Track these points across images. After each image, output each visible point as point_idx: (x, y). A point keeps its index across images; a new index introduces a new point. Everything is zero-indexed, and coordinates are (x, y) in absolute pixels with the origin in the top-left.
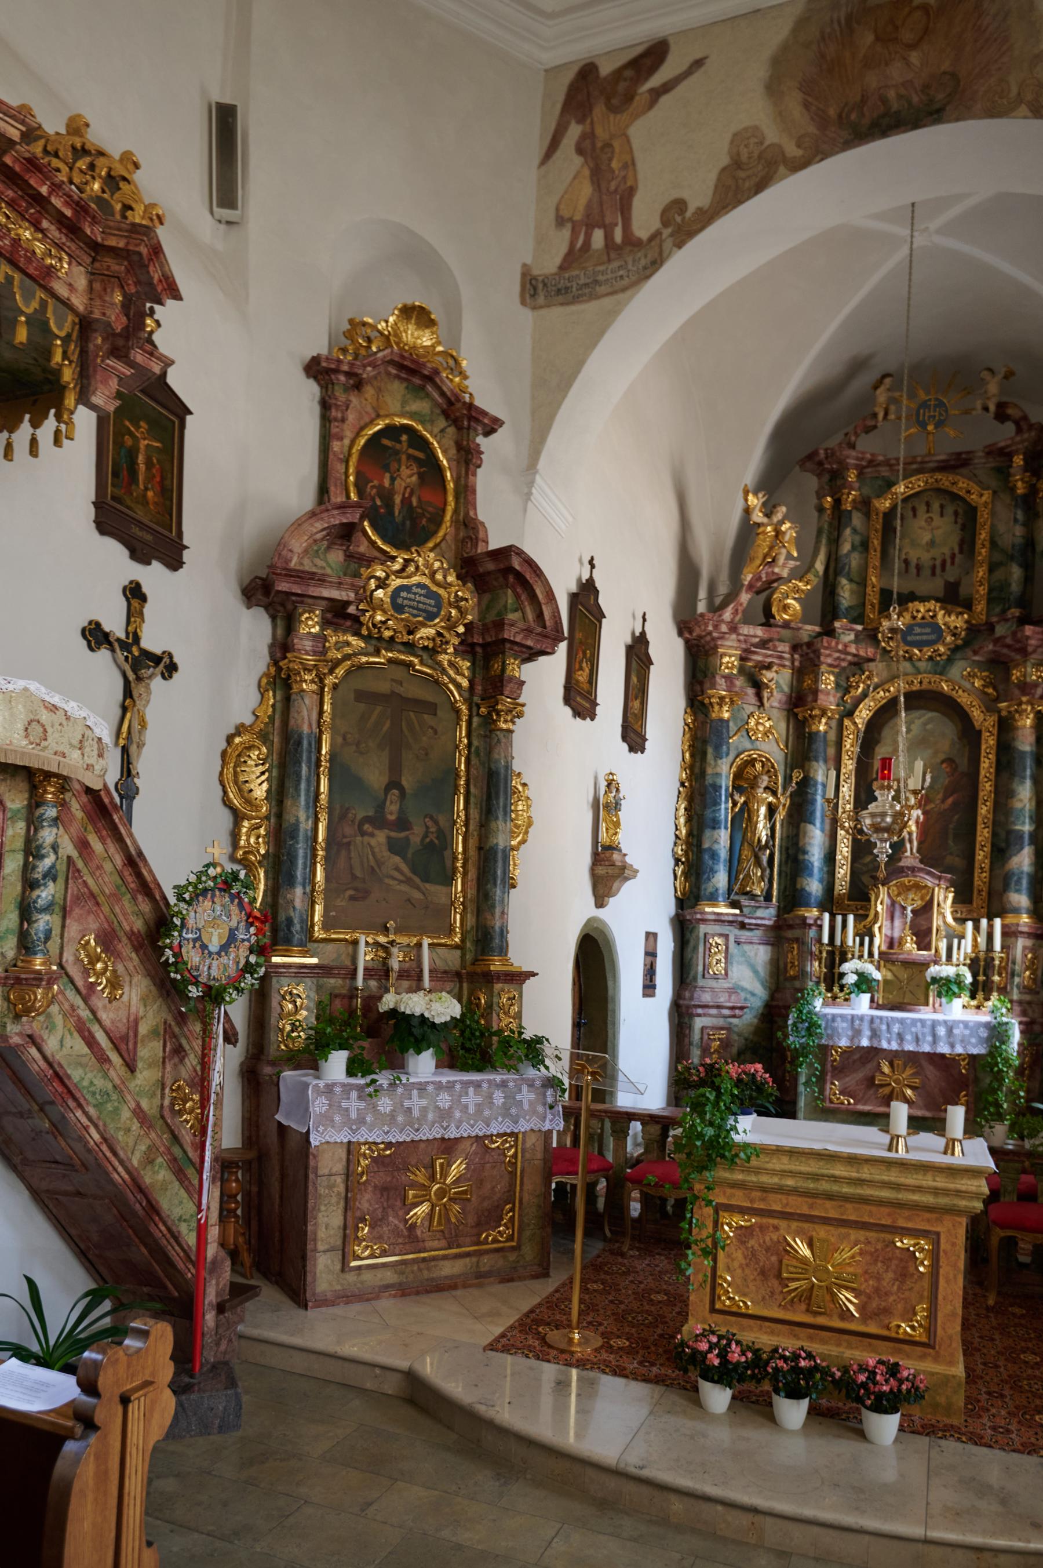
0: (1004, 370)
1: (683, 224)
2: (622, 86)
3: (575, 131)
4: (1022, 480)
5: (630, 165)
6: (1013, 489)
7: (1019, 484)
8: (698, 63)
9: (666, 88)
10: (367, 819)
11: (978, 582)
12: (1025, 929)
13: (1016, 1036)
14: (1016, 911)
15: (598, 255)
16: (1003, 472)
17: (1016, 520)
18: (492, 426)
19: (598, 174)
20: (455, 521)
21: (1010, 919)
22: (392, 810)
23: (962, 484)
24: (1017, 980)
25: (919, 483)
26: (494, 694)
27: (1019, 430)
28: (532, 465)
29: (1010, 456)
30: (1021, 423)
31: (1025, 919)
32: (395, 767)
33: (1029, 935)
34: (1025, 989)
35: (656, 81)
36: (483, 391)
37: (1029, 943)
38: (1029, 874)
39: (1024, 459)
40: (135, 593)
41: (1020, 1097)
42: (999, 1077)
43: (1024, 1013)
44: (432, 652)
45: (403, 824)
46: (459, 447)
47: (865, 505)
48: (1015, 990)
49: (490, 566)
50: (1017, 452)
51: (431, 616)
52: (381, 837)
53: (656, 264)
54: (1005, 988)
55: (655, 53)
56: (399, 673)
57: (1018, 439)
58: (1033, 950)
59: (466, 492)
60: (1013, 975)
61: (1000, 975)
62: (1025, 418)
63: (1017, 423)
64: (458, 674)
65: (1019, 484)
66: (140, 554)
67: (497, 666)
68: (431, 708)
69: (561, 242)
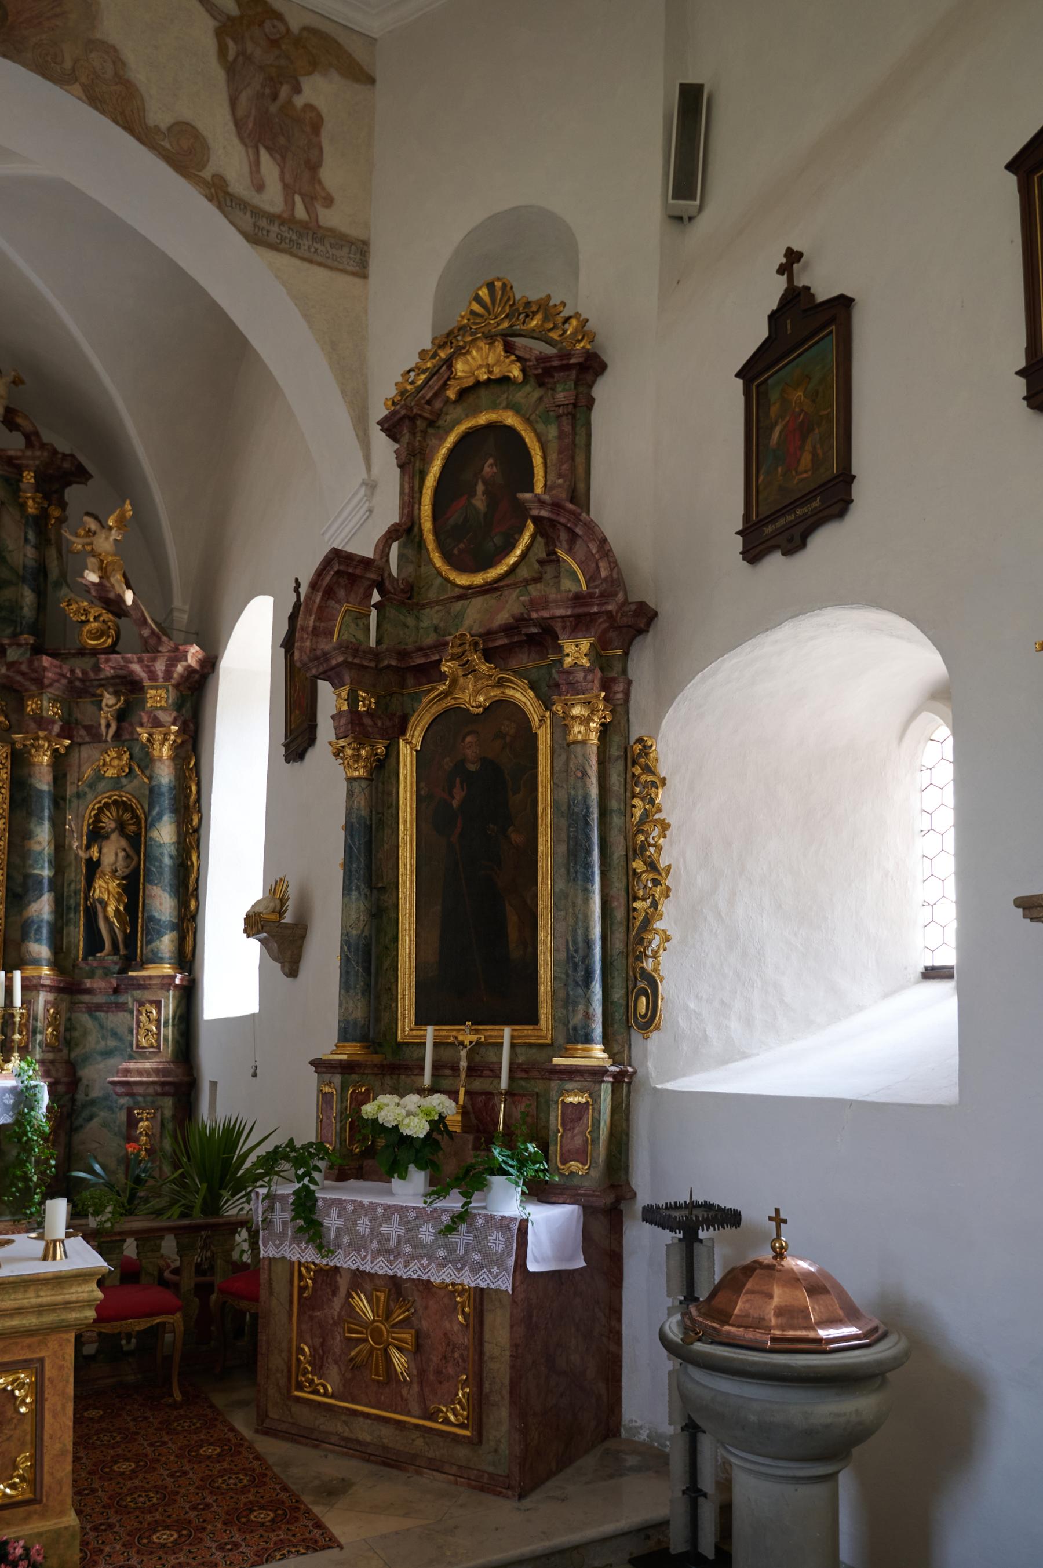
0: (13, 373)
4: (34, 499)
6: (23, 506)
7: (30, 502)
12: (48, 982)
13: (44, 1099)
14: (36, 962)
17: (26, 540)
24: (39, 1037)
27: (29, 444)
29: (19, 469)
30: (31, 439)
31: (46, 971)
33: (51, 989)
34: (48, 1047)
37: (51, 997)
38: (48, 923)
39: (35, 477)
41: (51, 1167)
42: (27, 1148)
43: (46, 1074)
48: (38, 1048)
50: (27, 467)
54: (26, 1047)
57: (29, 453)
58: (55, 1004)
60: (34, 1032)
61: (20, 1033)
62: (37, 434)
63: (27, 437)
65: (30, 502)
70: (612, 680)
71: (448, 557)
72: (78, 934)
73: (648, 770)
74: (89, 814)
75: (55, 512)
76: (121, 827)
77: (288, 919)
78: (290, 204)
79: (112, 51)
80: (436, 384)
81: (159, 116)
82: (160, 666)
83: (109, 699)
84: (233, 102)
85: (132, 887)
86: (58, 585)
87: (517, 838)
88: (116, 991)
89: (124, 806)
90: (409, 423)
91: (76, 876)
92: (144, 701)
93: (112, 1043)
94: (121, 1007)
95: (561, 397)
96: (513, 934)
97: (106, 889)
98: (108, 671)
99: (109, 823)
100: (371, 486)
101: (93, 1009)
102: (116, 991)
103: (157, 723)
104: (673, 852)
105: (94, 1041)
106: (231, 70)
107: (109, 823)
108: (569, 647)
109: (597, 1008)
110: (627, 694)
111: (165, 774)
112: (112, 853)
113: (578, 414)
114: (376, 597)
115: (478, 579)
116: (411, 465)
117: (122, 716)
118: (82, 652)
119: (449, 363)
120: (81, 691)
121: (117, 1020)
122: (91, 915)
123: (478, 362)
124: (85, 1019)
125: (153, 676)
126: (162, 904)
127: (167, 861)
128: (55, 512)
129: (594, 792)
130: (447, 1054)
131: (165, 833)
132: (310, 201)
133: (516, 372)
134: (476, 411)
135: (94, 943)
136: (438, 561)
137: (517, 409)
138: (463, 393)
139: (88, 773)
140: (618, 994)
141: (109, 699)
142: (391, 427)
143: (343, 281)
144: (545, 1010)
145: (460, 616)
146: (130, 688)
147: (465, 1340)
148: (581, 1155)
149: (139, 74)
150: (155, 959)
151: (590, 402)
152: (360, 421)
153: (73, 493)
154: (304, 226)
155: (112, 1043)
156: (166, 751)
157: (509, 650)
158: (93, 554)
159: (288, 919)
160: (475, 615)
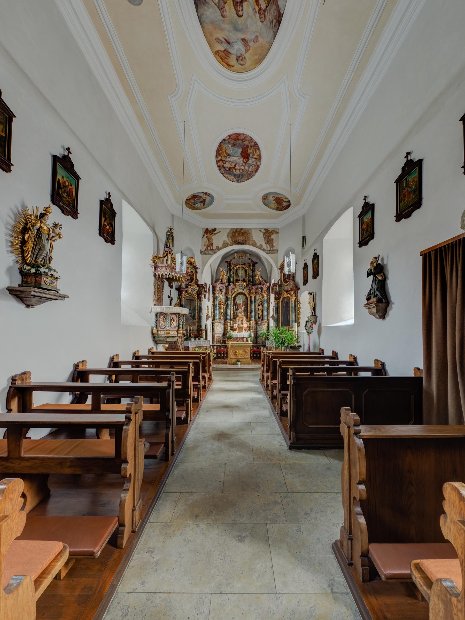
1: (218, 249)
3: (206, 235)
5: (212, 241)
9: (216, 233)
11: (247, 279)
15: (209, 249)
16: (249, 266)
19: (209, 241)
23: (245, 267)
25: (240, 266)
26: (200, 298)
28: (202, 273)
30: (252, 261)
36: (198, 264)
40: (170, 292)
47: (233, 268)
53: (216, 252)
55: (215, 230)
59: (196, 276)
64: (196, 297)
66: (171, 288)
68: (193, 300)
69: (205, 248)
72: (257, 317)
81: (258, 245)
85: (262, 311)
91: (257, 310)
97: (260, 312)
100: (278, 274)
101: (259, 325)
105: (259, 329)
106: (265, 238)
111: (266, 298)
112: (260, 307)
117: (261, 291)
118: (257, 284)
120: (257, 289)
121: (261, 326)
122: (258, 314)
126: (265, 313)
131: (266, 305)
132: (272, 247)
135: (259, 318)
142: (279, 269)
143: (276, 254)
146: (262, 288)
149: (256, 242)
152: (277, 267)
153: (256, 265)
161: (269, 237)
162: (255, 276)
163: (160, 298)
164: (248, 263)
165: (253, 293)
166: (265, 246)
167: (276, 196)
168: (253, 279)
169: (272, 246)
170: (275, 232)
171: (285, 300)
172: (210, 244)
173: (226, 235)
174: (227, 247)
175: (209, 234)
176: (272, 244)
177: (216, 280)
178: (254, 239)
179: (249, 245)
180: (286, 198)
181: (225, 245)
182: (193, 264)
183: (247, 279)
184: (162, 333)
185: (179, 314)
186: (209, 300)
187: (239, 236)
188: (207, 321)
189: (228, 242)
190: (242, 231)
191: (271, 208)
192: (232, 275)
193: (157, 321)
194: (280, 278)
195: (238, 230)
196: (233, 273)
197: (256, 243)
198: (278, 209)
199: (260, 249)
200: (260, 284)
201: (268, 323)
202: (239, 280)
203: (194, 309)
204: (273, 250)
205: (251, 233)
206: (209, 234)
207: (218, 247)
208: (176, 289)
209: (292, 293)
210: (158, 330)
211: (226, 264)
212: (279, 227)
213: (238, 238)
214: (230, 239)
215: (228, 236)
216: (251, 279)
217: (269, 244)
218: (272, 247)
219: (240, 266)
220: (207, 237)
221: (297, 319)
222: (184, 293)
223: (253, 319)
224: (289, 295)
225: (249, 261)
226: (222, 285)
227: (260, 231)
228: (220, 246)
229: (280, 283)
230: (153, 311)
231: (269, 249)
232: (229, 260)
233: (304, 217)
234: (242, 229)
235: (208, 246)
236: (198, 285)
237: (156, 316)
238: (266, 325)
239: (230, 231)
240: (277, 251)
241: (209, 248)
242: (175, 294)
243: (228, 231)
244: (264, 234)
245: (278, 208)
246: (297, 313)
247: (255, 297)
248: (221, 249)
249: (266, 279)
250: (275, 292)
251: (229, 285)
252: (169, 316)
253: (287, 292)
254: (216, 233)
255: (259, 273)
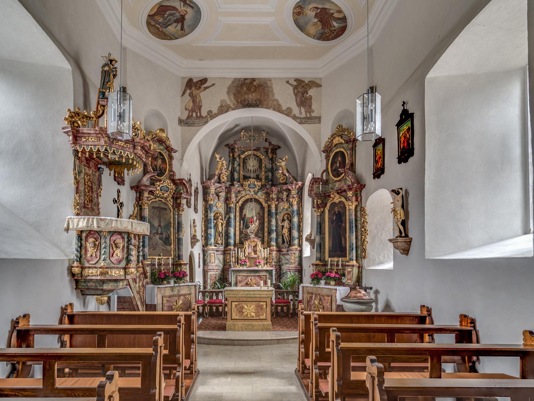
1: (212, 116)
2: (198, 85)
3: (188, 91)
5: (200, 101)
8: (214, 84)
9: (207, 88)
10: (155, 233)
11: (263, 175)
14: (273, 246)
15: (194, 118)
16: (267, 152)
18: (175, 152)
19: (194, 101)
20: (169, 170)
21: (272, 248)
22: (160, 231)
23: (259, 154)
26: (177, 206)
27: (269, 145)
28: (182, 159)
29: (268, 149)
30: (270, 143)
32: (160, 222)
35: (205, 85)
36: (174, 143)
40: (119, 191)
44: (166, 198)
45: (162, 234)
46: (169, 156)
47: (239, 156)
49: (178, 182)
51: (167, 192)
52: (158, 236)
53: (207, 122)
55: (204, 81)
56: (160, 202)
59: (171, 165)
64: (170, 203)
67: (179, 201)
68: (166, 209)
69: (186, 113)
70: (358, 197)
71: (333, 175)
72: (280, 240)
73: (364, 213)
74: (282, 216)
75: (275, 156)
76: (288, 218)
77: (313, 238)
78: (306, 114)
79: (277, 100)
80: (330, 144)
81: (284, 108)
82: (294, 186)
83: (285, 193)
84: (296, 101)
85: (290, 230)
86: (275, 171)
87: (343, 225)
88: (288, 251)
89: (289, 214)
90: (327, 150)
91: (280, 228)
92: (291, 193)
93: (287, 261)
94: (288, 254)
95: (350, 147)
96: (343, 242)
97: (285, 231)
98: (284, 188)
99: (286, 218)
100: (321, 161)
102: (288, 251)
103: (294, 197)
104: (368, 227)
105: (284, 261)
106: (296, 95)
107: (286, 218)
108: (348, 193)
109: (354, 255)
110: (361, 199)
111: (295, 208)
112: (286, 224)
113: (353, 149)
114: (321, 183)
115: (338, 179)
116: (327, 157)
117: (287, 196)
118: (280, 184)
119: (332, 140)
120: (280, 192)
121: (288, 257)
122: (283, 236)
123: (336, 141)
124: (282, 257)
125: (292, 188)
126: (295, 234)
127: (296, 225)
128: (275, 156)
129: (354, 217)
130: (333, 263)
131: (295, 220)
132: (310, 113)
133: (343, 142)
134: (337, 148)
135: (283, 242)
136: (331, 175)
137: (343, 148)
138: (335, 146)
139: (282, 208)
140: (359, 252)
141: (285, 193)
142: (324, 151)
143: (316, 125)
144: (348, 255)
145: (335, 185)
146: (289, 191)
147: (330, 307)
148: (350, 279)
149: (281, 102)
150: (294, 245)
151: (356, 146)
152: (319, 149)
153: (278, 151)
154: (309, 117)
155: (287, 261)
156: (295, 203)
157: (341, 192)
158: (281, 166)
159: (313, 238)
160: (337, 185)
161: (303, 94)
162: (277, 170)
163: (91, 201)
164: (264, 148)
165: (273, 199)
166: (296, 111)
167: (320, 6)
168: (273, 176)
169: (309, 109)
170: (314, 84)
171: (336, 209)
172: (197, 106)
173: (225, 90)
174: (227, 111)
175: (193, 88)
176: (310, 106)
177: (209, 175)
178: (277, 96)
179: (267, 108)
180: (340, 11)
181: (223, 109)
182: (164, 142)
183: (263, 175)
184: (93, 273)
185: (128, 234)
186: (196, 210)
187: (250, 92)
188: (192, 247)
189: (228, 102)
190: (255, 83)
191: (308, 35)
192: (237, 168)
193: (81, 247)
194: (325, 168)
195: (248, 81)
196: (239, 165)
197: (279, 105)
198: (323, 37)
199: (287, 115)
200: (286, 183)
201: (301, 252)
202: (250, 178)
203: (168, 226)
204: (311, 118)
205: (271, 87)
206: (193, 88)
207: (210, 112)
208: (132, 188)
209: (350, 194)
210: (83, 268)
211: (227, 150)
212: (321, 76)
213: (246, 97)
214: (232, 97)
215: (228, 93)
216: (270, 174)
217: (304, 106)
218: (310, 113)
219: (250, 152)
220: (191, 95)
221: (359, 243)
222: (146, 194)
223: (273, 243)
224: (343, 199)
225: (267, 145)
226: (219, 185)
227: (288, 82)
228: (215, 111)
229: (324, 178)
230: (71, 227)
231: (303, 115)
232: (231, 142)
233: (370, 51)
234: (254, 80)
235: (193, 111)
236: (174, 181)
237: (80, 238)
238: (297, 253)
239: (233, 82)
240: (318, 119)
241: (194, 114)
242: (128, 196)
243: (229, 83)
244: (295, 88)
245: (322, 34)
246: (359, 233)
247: (277, 207)
248: (216, 115)
249: (295, 176)
250: (316, 194)
251: (233, 185)
252: (105, 237)
253: (341, 192)
254: (207, 88)
255: (283, 164)
